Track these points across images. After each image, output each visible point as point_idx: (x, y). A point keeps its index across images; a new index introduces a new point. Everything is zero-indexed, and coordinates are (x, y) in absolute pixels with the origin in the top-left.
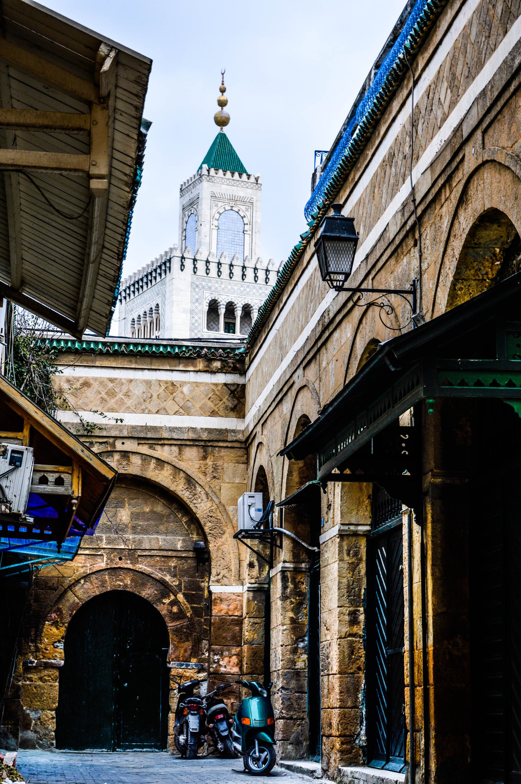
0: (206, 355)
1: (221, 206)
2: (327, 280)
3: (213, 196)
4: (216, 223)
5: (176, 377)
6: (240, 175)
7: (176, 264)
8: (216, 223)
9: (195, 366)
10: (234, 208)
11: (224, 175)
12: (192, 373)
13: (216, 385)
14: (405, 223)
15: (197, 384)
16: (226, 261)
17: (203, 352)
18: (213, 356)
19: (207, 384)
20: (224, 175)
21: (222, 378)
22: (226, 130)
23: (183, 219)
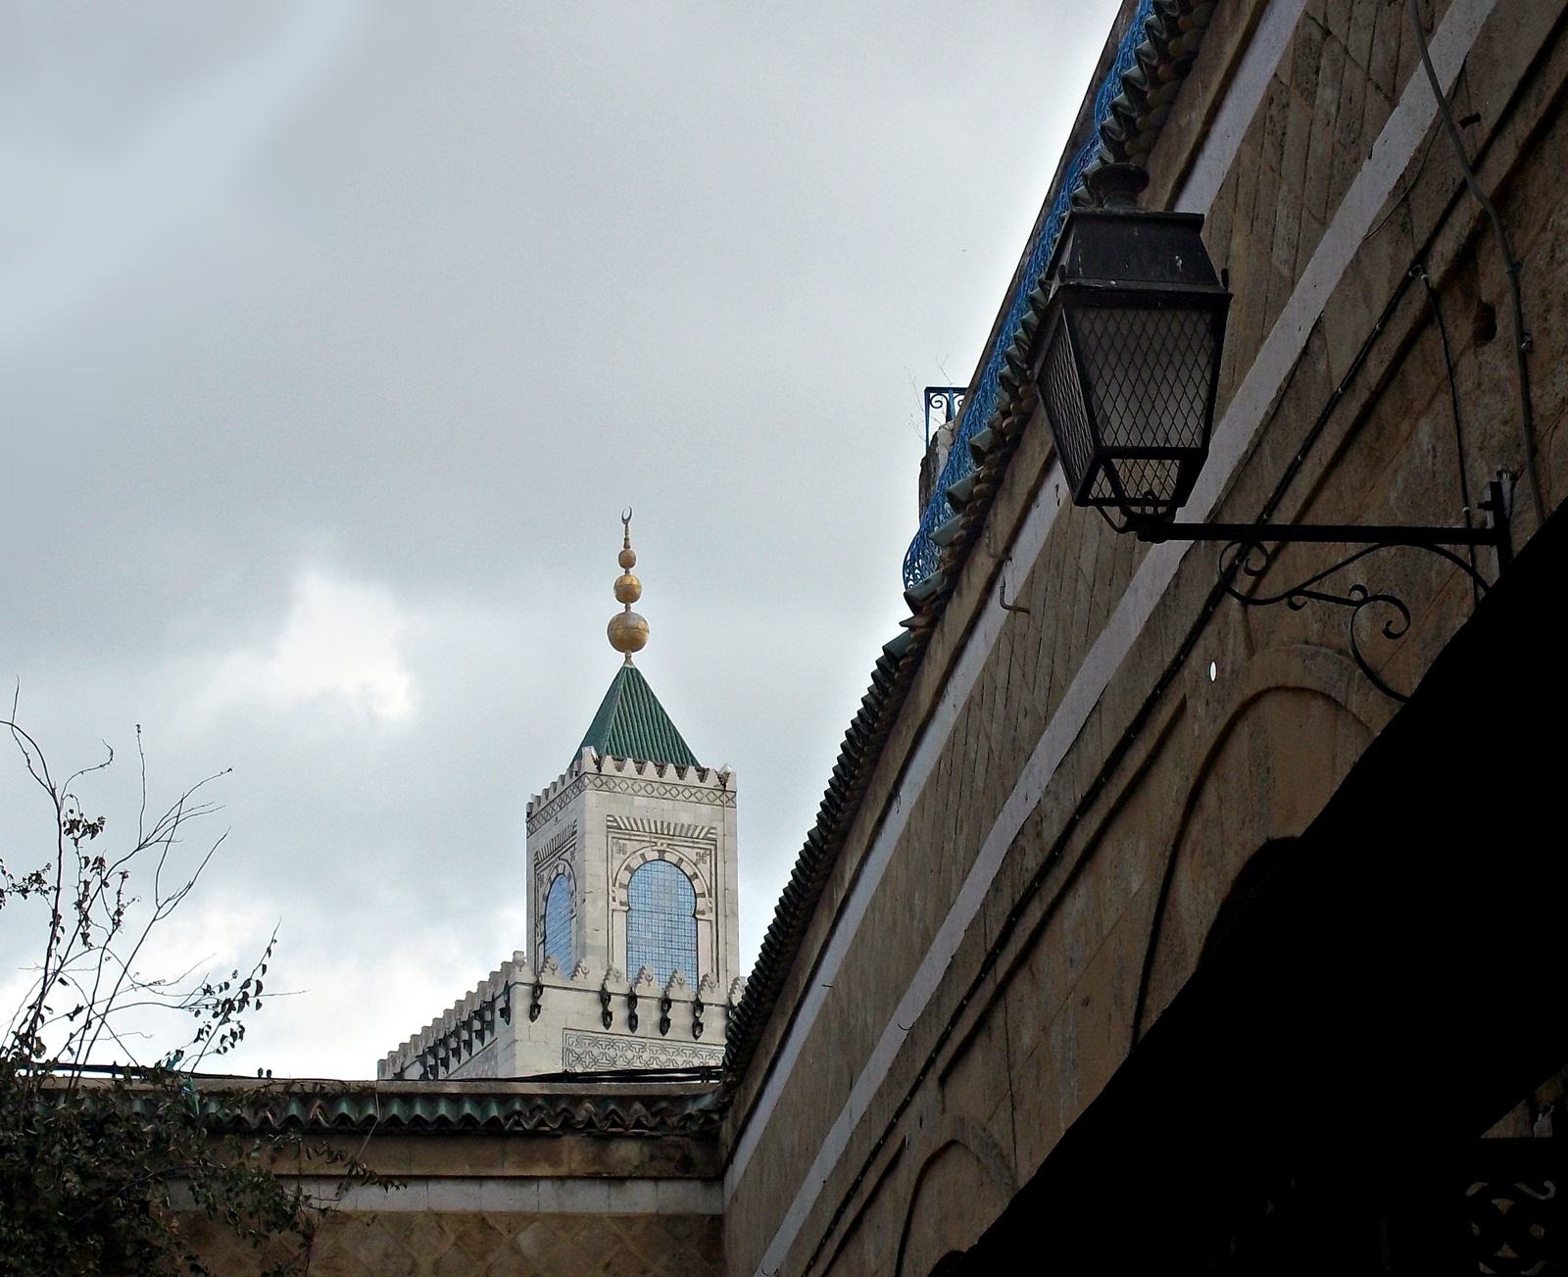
0: (590, 1123)
1: (637, 851)
2: (1099, 503)
3: (613, 827)
4: (622, 895)
5: (494, 1199)
6: (681, 772)
7: (520, 1004)
8: (622, 895)
9: (555, 1163)
10: (667, 857)
11: (640, 771)
12: (546, 1187)
13: (627, 1220)
14: (1422, 258)
15: (566, 1220)
16: (650, 991)
17: (581, 1115)
18: (614, 1124)
19: (594, 1219)
20: (640, 771)
21: (644, 1198)
22: (638, 659)
23: (536, 890)
